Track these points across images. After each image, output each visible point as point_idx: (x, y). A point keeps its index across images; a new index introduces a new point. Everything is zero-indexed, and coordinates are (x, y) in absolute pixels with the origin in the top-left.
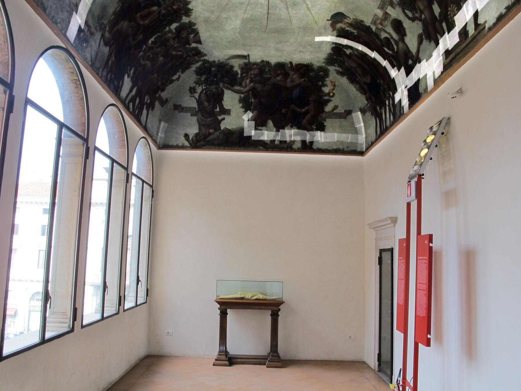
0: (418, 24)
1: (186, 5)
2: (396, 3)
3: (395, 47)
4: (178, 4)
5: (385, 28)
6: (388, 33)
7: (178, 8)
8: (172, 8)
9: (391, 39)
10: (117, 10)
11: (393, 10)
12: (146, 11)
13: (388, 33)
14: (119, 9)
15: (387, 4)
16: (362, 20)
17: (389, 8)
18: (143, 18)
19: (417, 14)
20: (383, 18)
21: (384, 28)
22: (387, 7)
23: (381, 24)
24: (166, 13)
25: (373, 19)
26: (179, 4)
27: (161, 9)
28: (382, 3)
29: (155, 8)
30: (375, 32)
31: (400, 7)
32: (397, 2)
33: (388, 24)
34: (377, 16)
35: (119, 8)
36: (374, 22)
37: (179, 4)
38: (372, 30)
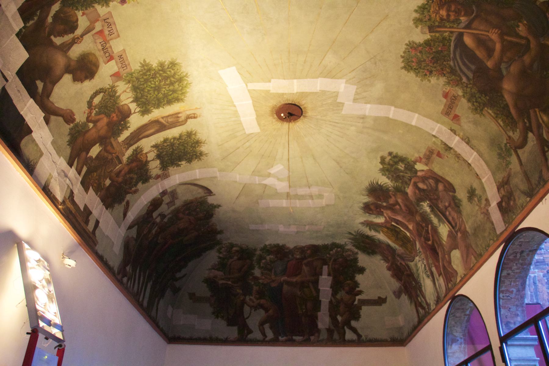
0: (85, 113)
1: (427, 6)
2: (116, 84)
3: (58, 41)
4: (436, 16)
5: (93, 35)
6: (82, 36)
7: (441, 6)
8: (448, 15)
9: (71, 36)
10: (493, 114)
11: (112, 72)
12: (480, 54)
13: (82, 36)
14: (491, 110)
15: (121, 70)
16: (125, 5)
17: (115, 69)
18: (490, 52)
19: (96, 115)
20: (108, 45)
21: (94, 32)
22: (118, 67)
23: (101, 32)
24: (463, 13)
25: (115, 24)
26: (434, 15)
27: (464, 28)
28: (126, 63)
29: (468, 40)
30: (93, 7)
31: (108, 87)
32: (117, 86)
33: (96, 48)
34: (116, 38)
35: (490, 112)
36: (108, 21)
37: (433, 16)
38: (99, 4)
